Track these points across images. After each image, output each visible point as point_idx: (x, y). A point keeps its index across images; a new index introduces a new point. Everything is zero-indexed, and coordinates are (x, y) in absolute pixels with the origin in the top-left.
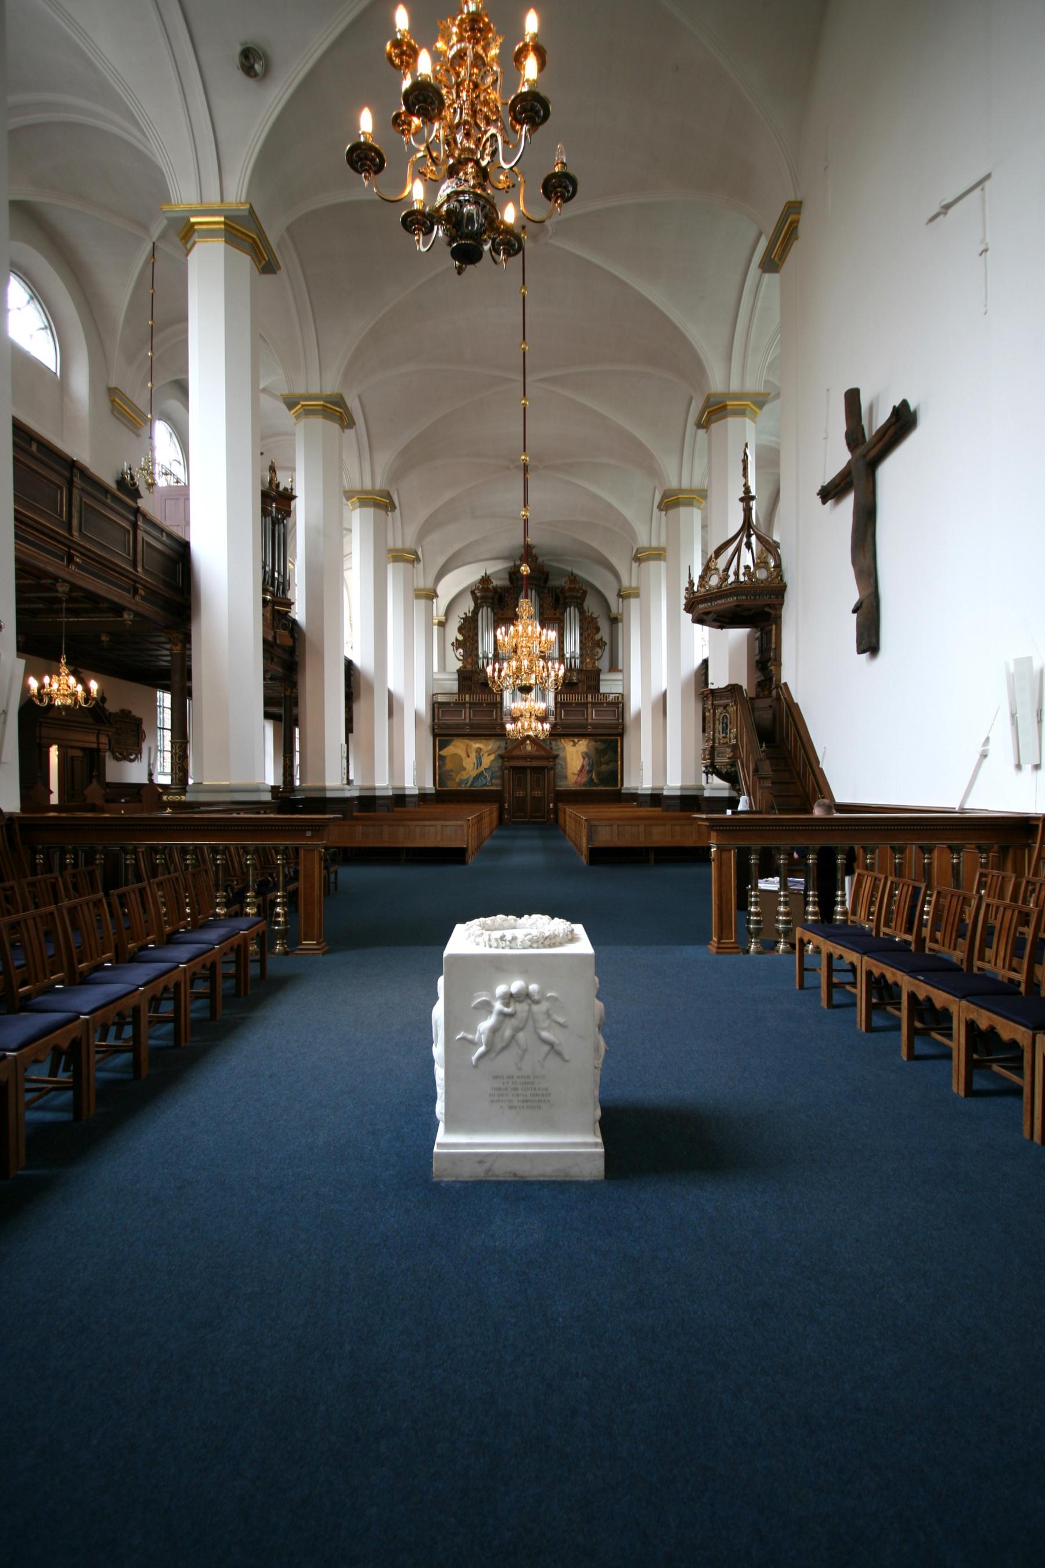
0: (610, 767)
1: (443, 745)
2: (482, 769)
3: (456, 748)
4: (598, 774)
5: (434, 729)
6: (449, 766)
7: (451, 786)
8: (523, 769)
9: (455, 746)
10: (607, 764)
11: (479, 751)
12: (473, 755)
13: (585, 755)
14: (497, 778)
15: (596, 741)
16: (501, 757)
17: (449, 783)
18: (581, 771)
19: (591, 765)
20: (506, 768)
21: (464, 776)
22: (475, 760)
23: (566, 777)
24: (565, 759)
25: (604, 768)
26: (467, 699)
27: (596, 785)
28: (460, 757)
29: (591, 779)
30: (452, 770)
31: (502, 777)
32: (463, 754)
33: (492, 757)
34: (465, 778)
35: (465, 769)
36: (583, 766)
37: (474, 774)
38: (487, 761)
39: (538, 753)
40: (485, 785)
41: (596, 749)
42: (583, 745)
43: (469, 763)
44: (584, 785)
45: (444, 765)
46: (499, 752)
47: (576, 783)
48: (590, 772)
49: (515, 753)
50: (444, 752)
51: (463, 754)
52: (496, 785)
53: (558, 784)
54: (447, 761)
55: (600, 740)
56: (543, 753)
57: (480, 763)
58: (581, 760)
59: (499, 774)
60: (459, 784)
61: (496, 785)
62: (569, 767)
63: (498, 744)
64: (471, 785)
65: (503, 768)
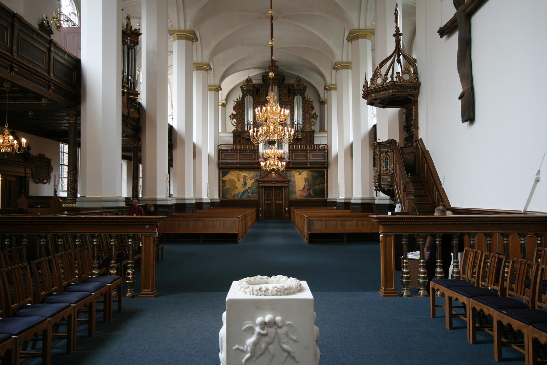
0: (321, 186)
1: (224, 174)
2: (246, 188)
3: (232, 176)
4: (313, 191)
6: (228, 186)
8: (271, 187)
10: (319, 185)
11: (245, 177)
12: (242, 180)
13: (306, 180)
14: (255, 193)
15: (312, 172)
18: (304, 189)
19: (310, 185)
20: (260, 187)
21: (236, 192)
22: (243, 183)
23: (295, 192)
24: (294, 182)
25: (317, 187)
27: (313, 197)
28: (234, 181)
29: (310, 194)
30: (229, 189)
31: (259, 192)
32: (236, 180)
33: (253, 181)
35: (237, 188)
36: (305, 186)
37: (242, 190)
38: (250, 183)
40: (249, 197)
41: (313, 176)
42: (305, 174)
43: (239, 185)
44: (306, 197)
45: (225, 185)
46: (256, 178)
47: (301, 196)
48: (309, 189)
50: (225, 178)
51: (236, 180)
52: (255, 197)
53: (291, 196)
54: (227, 183)
55: (315, 171)
59: (257, 190)
61: (255, 197)
62: (297, 186)
63: (256, 173)
64: (240, 197)
65: (259, 188)
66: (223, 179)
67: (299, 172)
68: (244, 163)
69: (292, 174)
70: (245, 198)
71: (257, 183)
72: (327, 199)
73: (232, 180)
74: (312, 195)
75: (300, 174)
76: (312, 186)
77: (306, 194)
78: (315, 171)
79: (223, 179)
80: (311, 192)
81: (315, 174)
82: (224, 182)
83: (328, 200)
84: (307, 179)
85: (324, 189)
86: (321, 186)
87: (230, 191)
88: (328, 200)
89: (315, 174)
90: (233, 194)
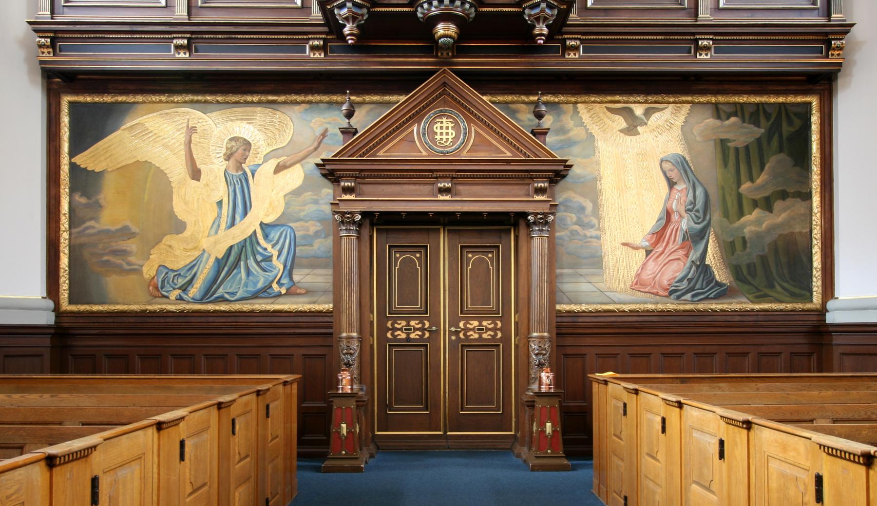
1: (90, 128)
2: (248, 226)
4: (729, 248)
6: (113, 213)
7: (125, 296)
10: (767, 204)
12: (215, 167)
13: (678, 171)
14: (313, 263)
15: (718, 112)
17: (113, 283)
18: (659, 235)
19: (702, 211)
21: (175, 253)
22: (221, 191)
23: (596, 261)
24: (592, 188)
25: (754, 222)
27: (724, 293)
28: (160, 174)
29: (703, 269)
30: (125, 233)
33: (295, 177)
34: (179, 259)
35: (179, 227)
40: (264, 292)
41: (723, 143)
45: (98, 206)
47: (639, 284)
48: (697, 237)
51: (175, 168)
53: (567, 286)
54: (108, 192)
55: (739, 110)
57: (241, 202)
59: (323, 245)
60: (157, 290)
64: (207, 294)
66: (83, 160)
67: (627, 113)
69: (576, 133)
70: (238, 296)
71: (327, 191)
72: (823, 311)
73: (143, 173)
74: (721, 275)
76: (716, 216)
77: (674, 268)
78: (739, 110)
79: (83, 160)
80: (710, 260)
81: (741, 133)
82: (85, 181)
83: (831, 318)
84: (682, 164)
86: (782, 215)
87: (132, 245)
88: (831, 318)
89: (741, 133)
90: (149, 271)
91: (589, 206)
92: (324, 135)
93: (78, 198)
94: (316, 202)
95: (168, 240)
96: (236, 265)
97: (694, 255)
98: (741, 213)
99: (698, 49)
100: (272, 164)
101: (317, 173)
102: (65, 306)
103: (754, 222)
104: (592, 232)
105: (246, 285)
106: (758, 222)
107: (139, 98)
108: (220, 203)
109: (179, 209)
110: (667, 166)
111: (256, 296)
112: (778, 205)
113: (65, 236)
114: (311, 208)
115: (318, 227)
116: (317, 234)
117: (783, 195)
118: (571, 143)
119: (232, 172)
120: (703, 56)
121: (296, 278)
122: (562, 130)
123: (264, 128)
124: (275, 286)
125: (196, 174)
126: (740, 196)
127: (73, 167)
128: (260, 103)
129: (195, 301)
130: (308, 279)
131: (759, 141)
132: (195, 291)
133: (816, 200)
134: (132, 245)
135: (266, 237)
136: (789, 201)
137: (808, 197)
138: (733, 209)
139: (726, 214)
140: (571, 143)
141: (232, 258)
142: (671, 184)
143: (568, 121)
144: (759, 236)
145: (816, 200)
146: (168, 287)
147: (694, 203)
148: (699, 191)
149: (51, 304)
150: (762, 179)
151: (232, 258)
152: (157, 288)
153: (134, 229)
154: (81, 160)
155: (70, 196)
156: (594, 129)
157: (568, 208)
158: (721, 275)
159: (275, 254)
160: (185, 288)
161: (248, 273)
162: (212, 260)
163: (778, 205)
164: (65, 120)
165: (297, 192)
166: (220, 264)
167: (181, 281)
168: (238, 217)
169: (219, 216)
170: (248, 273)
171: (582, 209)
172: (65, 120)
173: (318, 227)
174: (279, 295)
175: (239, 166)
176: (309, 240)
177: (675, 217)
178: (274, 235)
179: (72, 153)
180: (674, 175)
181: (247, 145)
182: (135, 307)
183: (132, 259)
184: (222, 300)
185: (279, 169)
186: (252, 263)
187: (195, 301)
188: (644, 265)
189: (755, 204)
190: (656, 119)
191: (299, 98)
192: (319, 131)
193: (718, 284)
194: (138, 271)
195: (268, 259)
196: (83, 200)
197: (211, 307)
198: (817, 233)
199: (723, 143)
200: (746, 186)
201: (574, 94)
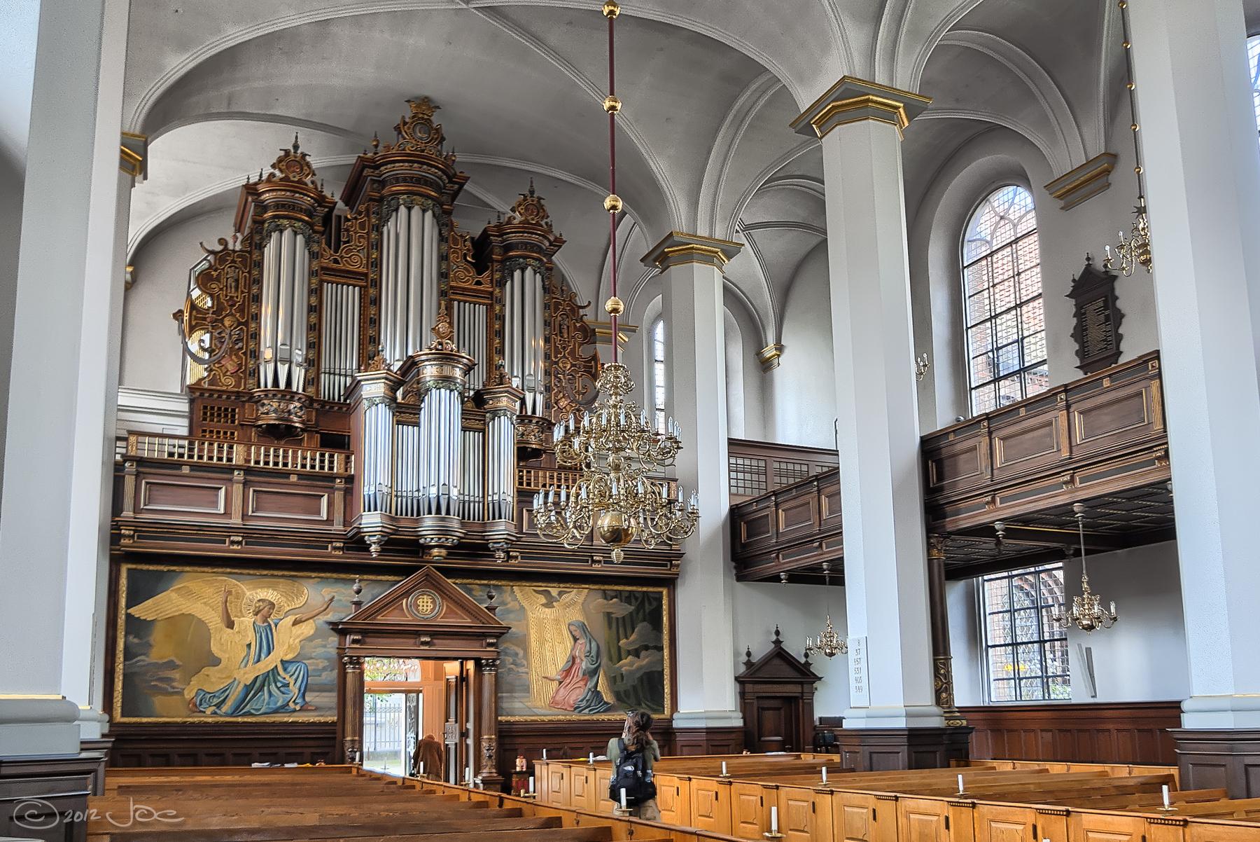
0: (645, 660)
2: (268, 663)
4: (612, 681)
5: (115, 538)
6: (160, 650)
7: (168, 711)
9: (189, 593)
10: (636, 653)
11: (266, 611)
12: (246, 621)
13: (580, 632)
14: (322, 689)
16: (341, 630)
17: (158, 701)
18: (567, 672)
21: (213, 680)
22: (251, 637)
24: (523, 642)
25: (628, 664)
26: (238, 459)
30: (171, 665)
32: (213, 619)
33: (307, 629)
35: (216, 662)
37: (247, 676)
39: (452, 621)
40: (283, 709)
41: (608, 615)
42: (576, 605)
46: (331, 617)
47: (554, 703)
48: (593, 673)
49: (380, 619)
51: (213, 619)
53: (505, 705)
54: (157, 636)
56: (467, 621)
58: (569, 642)
60: (195, 708)
62: (535, 662)
64: (236, 710)
66: (136, 611)
68: (272, 537)
69: (512, 605)
70: (262, 710)
71: (334, 639)
75: (549, 605)
76: (604, 660)
77: (576, 693)
81: (621, 609)
82: (137, 627)
84: (583, 627)
85: (661, 673)
86: (645, 660)
89: (621, 609)
90: (189, 694)
91: (521, 653)
92: (332, 600)
93: (131, 638)
94: (325, 646)
95: (205, 671)
96: (261, 689)
97: (591, 684)
98: (620, 659)
99: (594, 561)
100: (290, 619)
101: (327, 627)
102: (118, 718)
103: (628, 664)
104: (523, 670)
105: (268, 704)
106: (631, 664)
107: (188, 569)
108: (249, 646)
109: (215, 649)
110: (572, 628)
111: (276, 711)
112: (643, 653)
113: (120, 668)
114: (321, 650)
115: (326, 663)
116: (324, 669)
117: (646, 648)
118: (509, 611)
119: (259, 623)
120: (596, 566)
121: (307, 699)
122: (504, 603)
123: (285, 595)
124: (291, 704)
125: (230, 625)
126: (619, 648)
127: (128, 616)
128: (283, 576)
129: (227, 715)
130: (317, 699)
131: (631, 613)
132: (225, 708)
133: (666, 652)
134: (176, 675)
135: (285, 670)
136: (650, 651)
137: (661, 649)
138: (615, 657)
139: (611, 659)
140: (509, 611)
141: (257, 684)
142: (576, 640)
143: (507, 597)
144: (631, 673)
145: (666, 652)
146: (204, 705)
147: (590, 652)
148: (594, 644)
149: (107, 717)
150: (632, 638)
151: (257, 684)
152: (195, 705)
153: (178, 662)
154: (136, 611)
155: (126, 636)
156: (525, 604)
157: (506, 654)
158: (608, 697)
159: (292, 683)
160: (219, 706)
161: (270, 694)
162: (242, 685)
163: (643, 653)
164: (123, 581)
165: (310, 639)
166: (248, 688)
167: (216, 701)
168: (263, 656)
169: (248, 654)
170: (270, 694)
171: (517, 654)
172: (123, 581)
173: (326, 663)
174: (295, 711)
175: (265, 621)
176: (319, 672)
177: (578, 661)
178: (292, 668)
179: (128, 607)
180: (577, 634)
181: (272, 605)
182: (179, 720)
183: (175, 684)
184: (249, 714)
185: (295, 623)
186: (273, 687)
187: (227, 715)
188: (558, 691)
189: (629, 653)
190: (566, 598)
191: (313, 575)
192: (327, 598)
193: (606, 703)
194: (181, 693)
195: (287, 685)
196: (136, 641)
197: (240, 719)
198: (667, 671)
199: (608, 615)
200: (623, 642)
201: (511, 580)
